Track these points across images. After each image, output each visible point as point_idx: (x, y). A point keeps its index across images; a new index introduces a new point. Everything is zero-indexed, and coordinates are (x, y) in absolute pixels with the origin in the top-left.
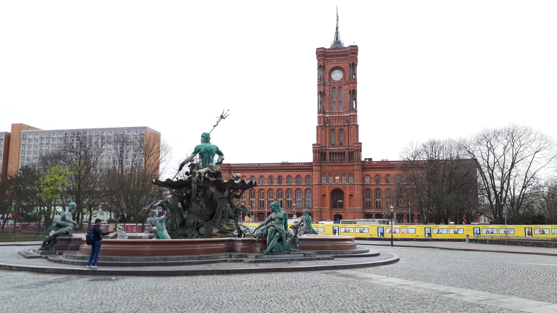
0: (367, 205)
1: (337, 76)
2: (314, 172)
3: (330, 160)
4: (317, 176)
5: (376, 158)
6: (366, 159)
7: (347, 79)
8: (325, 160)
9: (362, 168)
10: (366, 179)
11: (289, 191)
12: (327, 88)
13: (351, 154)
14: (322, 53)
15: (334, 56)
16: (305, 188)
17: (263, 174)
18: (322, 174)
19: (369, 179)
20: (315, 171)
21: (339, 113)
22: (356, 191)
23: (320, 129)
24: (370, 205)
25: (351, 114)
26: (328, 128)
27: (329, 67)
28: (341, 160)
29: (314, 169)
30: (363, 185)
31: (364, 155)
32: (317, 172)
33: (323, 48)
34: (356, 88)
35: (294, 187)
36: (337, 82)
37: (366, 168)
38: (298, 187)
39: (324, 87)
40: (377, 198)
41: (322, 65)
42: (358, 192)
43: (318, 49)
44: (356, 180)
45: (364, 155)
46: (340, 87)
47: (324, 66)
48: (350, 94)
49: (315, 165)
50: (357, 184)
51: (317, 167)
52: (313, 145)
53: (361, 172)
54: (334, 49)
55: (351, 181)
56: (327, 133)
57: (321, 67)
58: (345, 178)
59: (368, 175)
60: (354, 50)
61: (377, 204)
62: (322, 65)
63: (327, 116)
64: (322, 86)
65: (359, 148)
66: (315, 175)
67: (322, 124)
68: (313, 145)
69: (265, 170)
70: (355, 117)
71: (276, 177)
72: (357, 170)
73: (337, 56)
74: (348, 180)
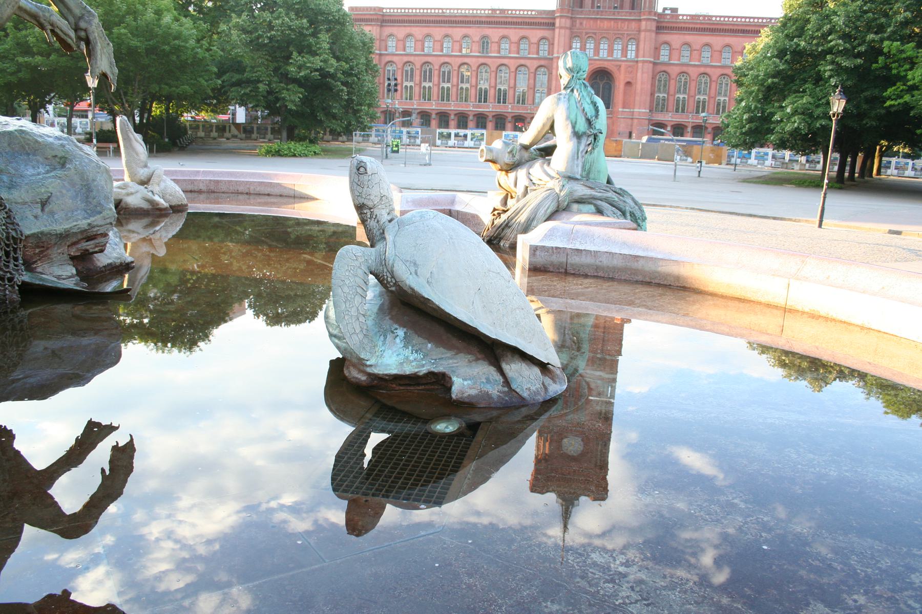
0: (658, 105)
2: (557, 31)
3: (593, 7)
4: (562, 39)
8: (581, 7)
9: (658, 28)
10: (662, 52)
11: (483, 69)
16: (536, 63)
17: (450, 31)
19: (667, 53)
20: (561, 28)
22: (639, 74)
24: (663, 105)
28: (615, 8)
29: (557, 25)
30: (654, 64)
32: (563, 31)
35: (512, 61)
38: (522, 62)
40: (679, 92)
42: (643, 79)
44: (641, 52)
49: (561, 17)
50: (644, 62)
51: (563, 20)
53: (653, 35)
55: (631, 55)
58: (620, 47)
59: (666, 43)
61: (678, 104)
66: (560, 36)
69: (456, 22)
71: (477, 39)
72: (646, 31)
74: (624, 51)
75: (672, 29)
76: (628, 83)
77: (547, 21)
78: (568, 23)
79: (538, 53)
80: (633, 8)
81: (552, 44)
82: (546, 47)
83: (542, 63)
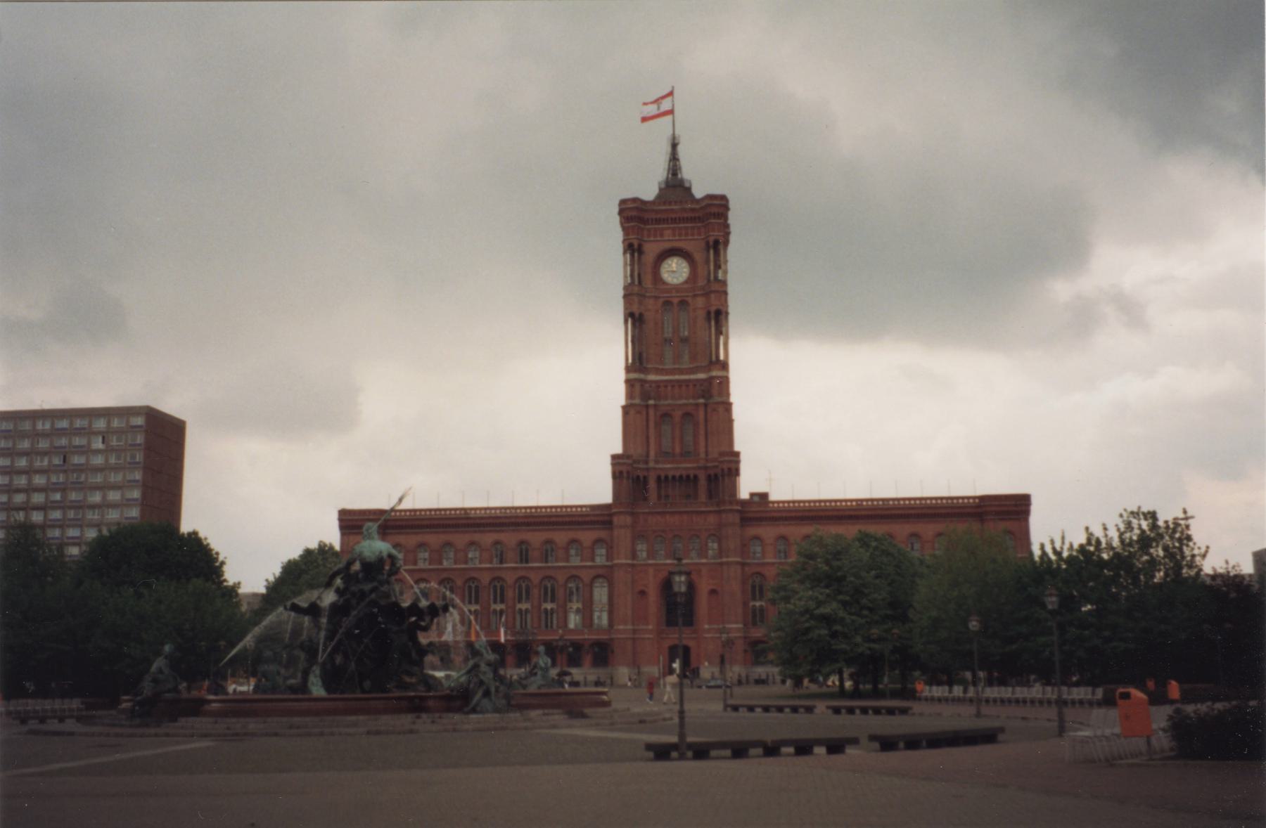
1: (675, 271)
2: (616, 532)
5: (780, 493)
6: (752, 495)
7: (701, 283)
12: (650, 303)
13: (713, 480)
14: (634, 213)
15: (665, 221)
17: (477, 537)
18: (638, 536)
21: (681, 372)
23: (632, 412)
25: (714, 373)
26: (651, 412)
27: (652, 250)
30: (743, 565)
31: (747, 486)
33: (635, 200)
34: (725, 303)
36: (677, 288)
37: (751, 519)
39: (640, 303)
41: (636, 243)
43: (623, 202)
45: (747, 486)
46: (683, 303)
47: (640, 246)
48: (709, 319)
52: (614, 457)
54: (665, 203)
56: (652, 424)
57: (633, 249)
59: (757, 538)
60: (717, 208)
62: (636, 243)
63: (652, 377)
64: (636, 299)
65: (733, 466)
66: (622, 536)
67: (637, 401)
68: (614, 457)
70: (725, 382)
73: (674, 221)
75: (760, 519)
76: (713, 592)
77: (601, 519)
78: (629, 520)
79: (593, 560)
80: (710, 496)
81: (610, 548)
82: (604, 551)
83: (600, 572)
